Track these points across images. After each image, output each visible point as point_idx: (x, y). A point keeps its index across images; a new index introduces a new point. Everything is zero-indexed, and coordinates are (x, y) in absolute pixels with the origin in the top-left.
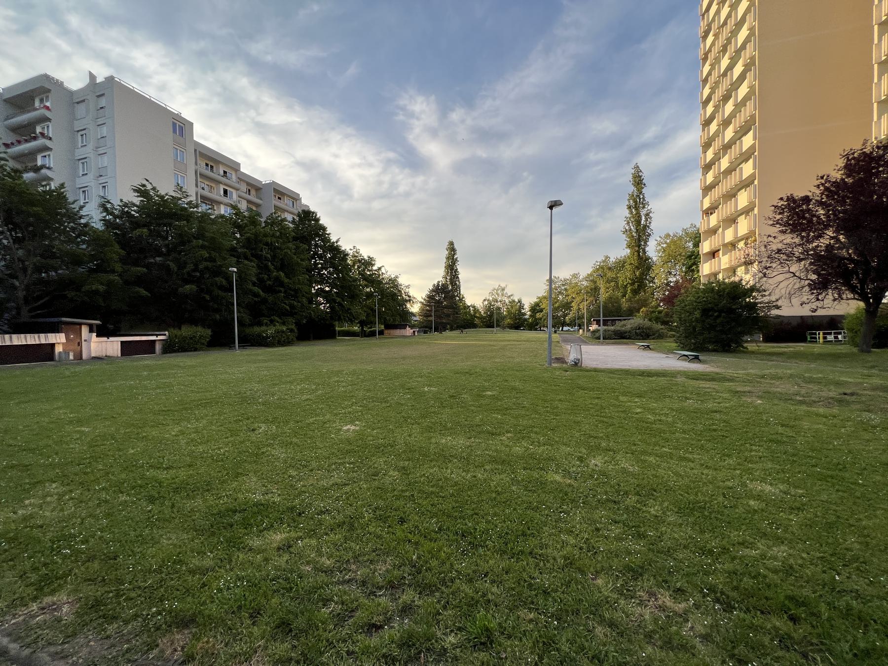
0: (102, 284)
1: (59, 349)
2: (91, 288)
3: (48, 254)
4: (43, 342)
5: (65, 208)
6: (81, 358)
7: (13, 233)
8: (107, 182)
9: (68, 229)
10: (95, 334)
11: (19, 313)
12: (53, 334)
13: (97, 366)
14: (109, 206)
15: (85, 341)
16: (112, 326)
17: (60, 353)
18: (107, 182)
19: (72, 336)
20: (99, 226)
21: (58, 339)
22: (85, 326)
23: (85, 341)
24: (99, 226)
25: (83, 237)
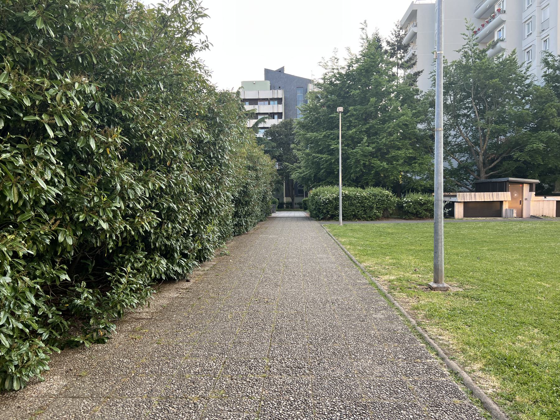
0: (542, 141)
1: (505, 206)
2: (533, 147)
3: (501, 120)
4: (495, 199)
5: (515, 74)
6: (522, 217)
7: (478, 107)
8: (548, 35)
9: (516, 93)
10: (534, 193)
11: (479, 175)
12: (502, 193)
13: (538, 224)
14: (550, 59)
15: (526, 199)
16: (547, 185)
17: (506, 209)
18: (548, 35)
19: (516, 195)
20: (540, 82)
21: (504, 196)
22: (527, 185)
23: (526, 199)
24: (540, 82)
25: (527, 98)
